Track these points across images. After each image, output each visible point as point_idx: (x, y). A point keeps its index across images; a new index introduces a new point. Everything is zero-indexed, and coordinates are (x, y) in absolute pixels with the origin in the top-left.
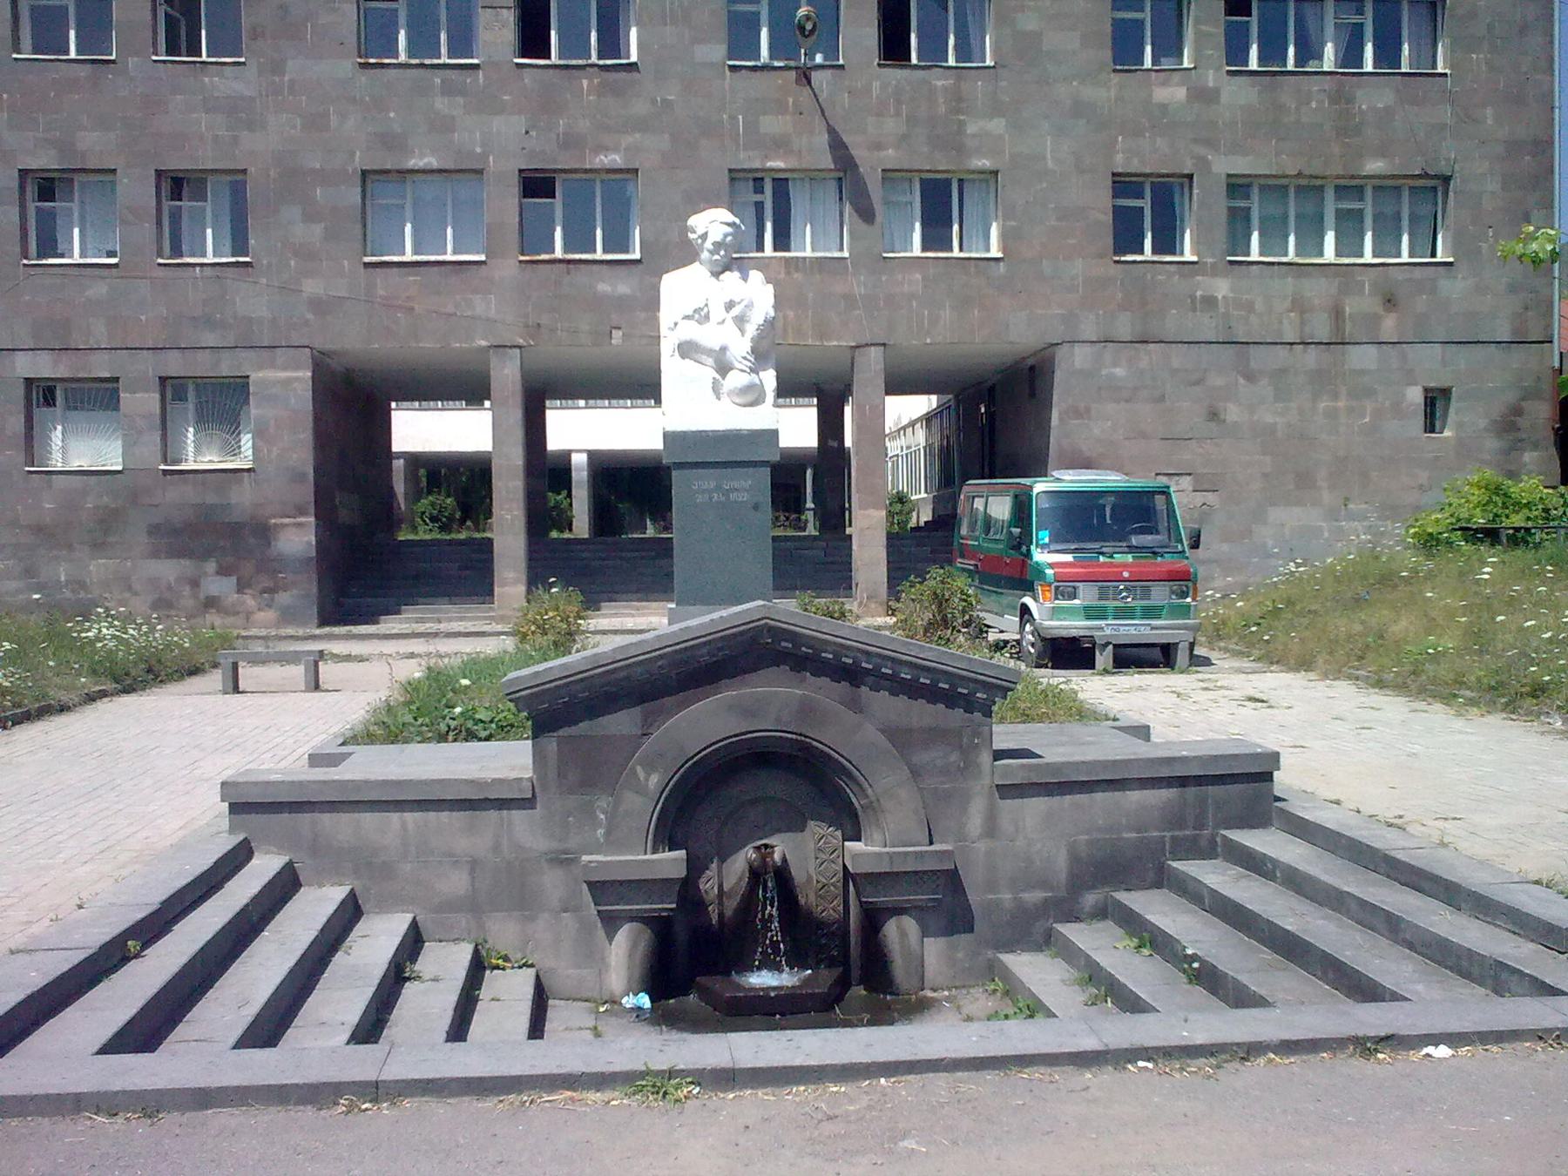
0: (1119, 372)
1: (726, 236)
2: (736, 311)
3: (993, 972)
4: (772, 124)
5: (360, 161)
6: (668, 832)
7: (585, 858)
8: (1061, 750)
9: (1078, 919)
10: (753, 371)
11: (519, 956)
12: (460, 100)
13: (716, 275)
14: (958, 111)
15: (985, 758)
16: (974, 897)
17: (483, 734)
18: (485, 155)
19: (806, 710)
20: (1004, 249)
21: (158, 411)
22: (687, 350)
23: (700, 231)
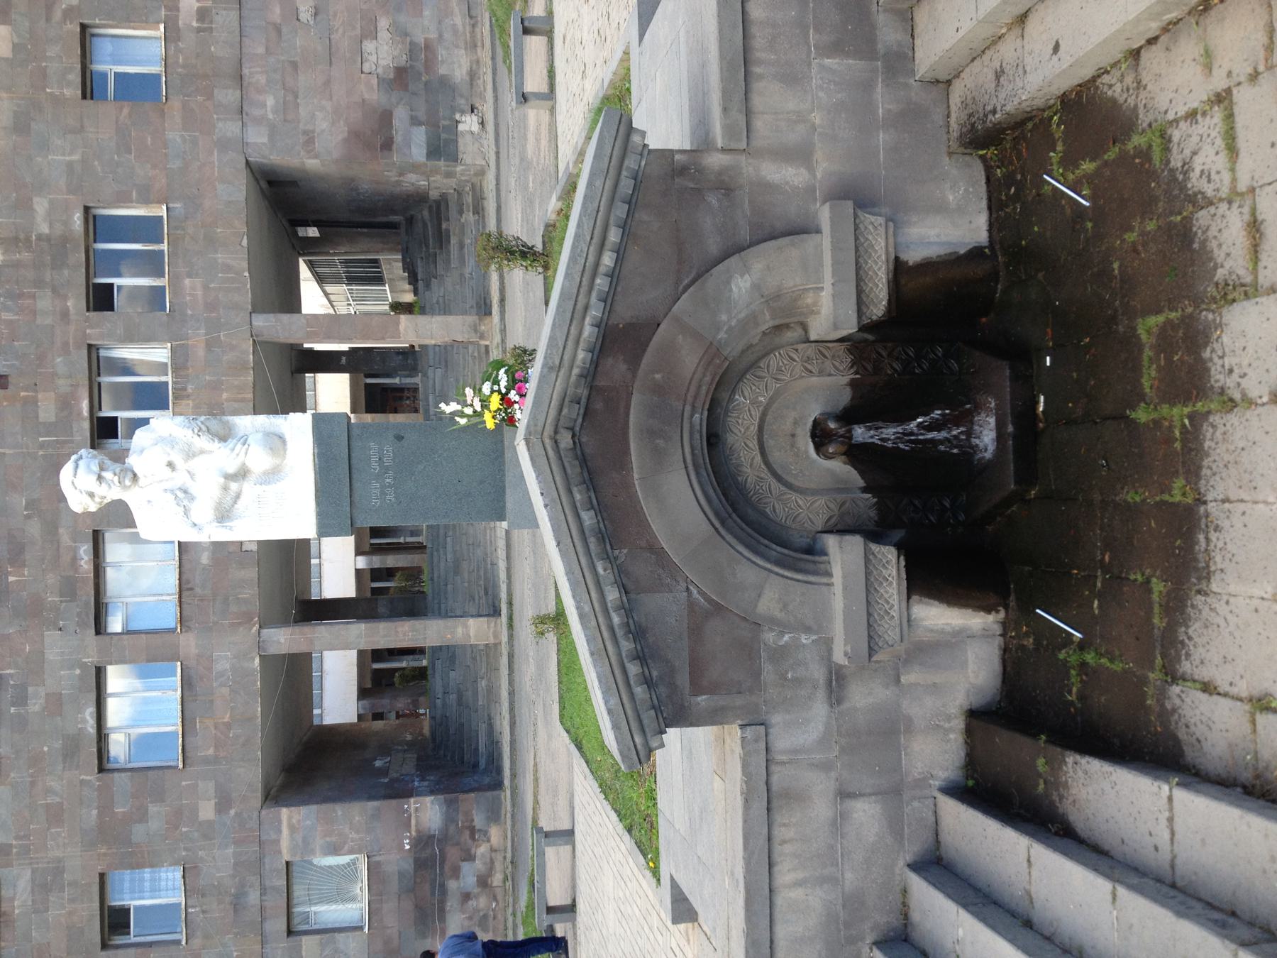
0: (270, 101)
4: (47, 410)
5: (91, 776)
12: (30, 689)
14: (28, 239)
18: (83, 666)
20: (160, 202)
21: (317, 937)
22: (223, 515)
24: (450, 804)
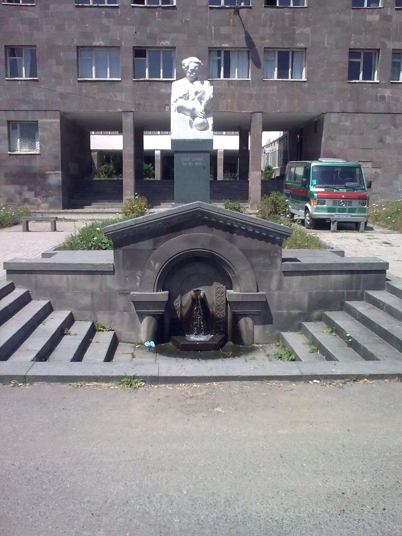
0: (347, 124)
1: (195, 67)
2: (198, 96)
3: (279, 338)
4: (224, 30)
5: (76, 42)
6: (162, 284)
7: (132, 293)
8: (309, 259)
9: (311, 321)
10: (204, 117)
11: (109, 327)
12: (112, 20)
13: (192, 82)
14: (293, 25)
15: (279, 261)
16: (273, 311)
17: (104, 247)
18: (120, 41)
19: (213, 241)
20: (307, 77)
21: (7, 132)
22: (180, 109)
23: (186, 65)
24: (58, 187)
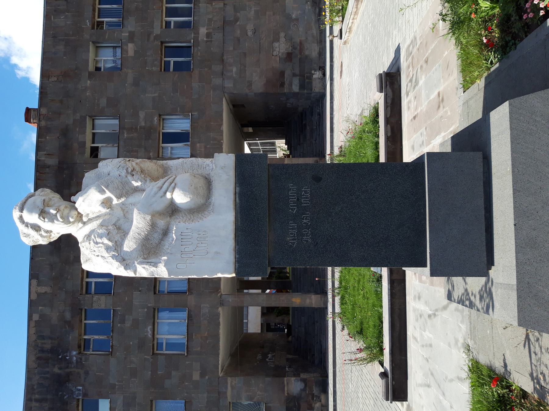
0: (234, 70)
12: (127, 317)
14: (136, 128)
18: (148, 308)
